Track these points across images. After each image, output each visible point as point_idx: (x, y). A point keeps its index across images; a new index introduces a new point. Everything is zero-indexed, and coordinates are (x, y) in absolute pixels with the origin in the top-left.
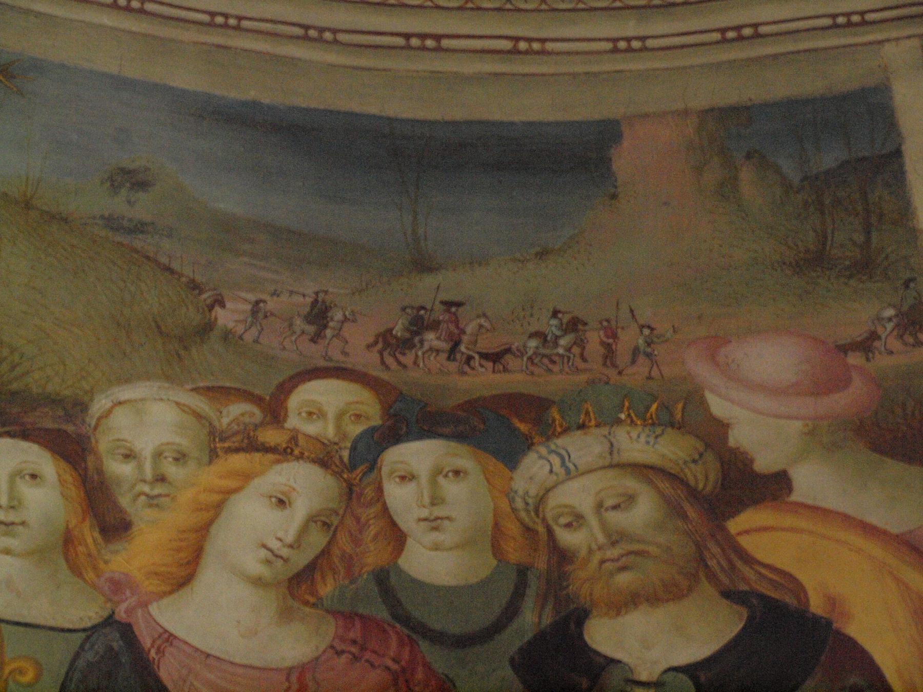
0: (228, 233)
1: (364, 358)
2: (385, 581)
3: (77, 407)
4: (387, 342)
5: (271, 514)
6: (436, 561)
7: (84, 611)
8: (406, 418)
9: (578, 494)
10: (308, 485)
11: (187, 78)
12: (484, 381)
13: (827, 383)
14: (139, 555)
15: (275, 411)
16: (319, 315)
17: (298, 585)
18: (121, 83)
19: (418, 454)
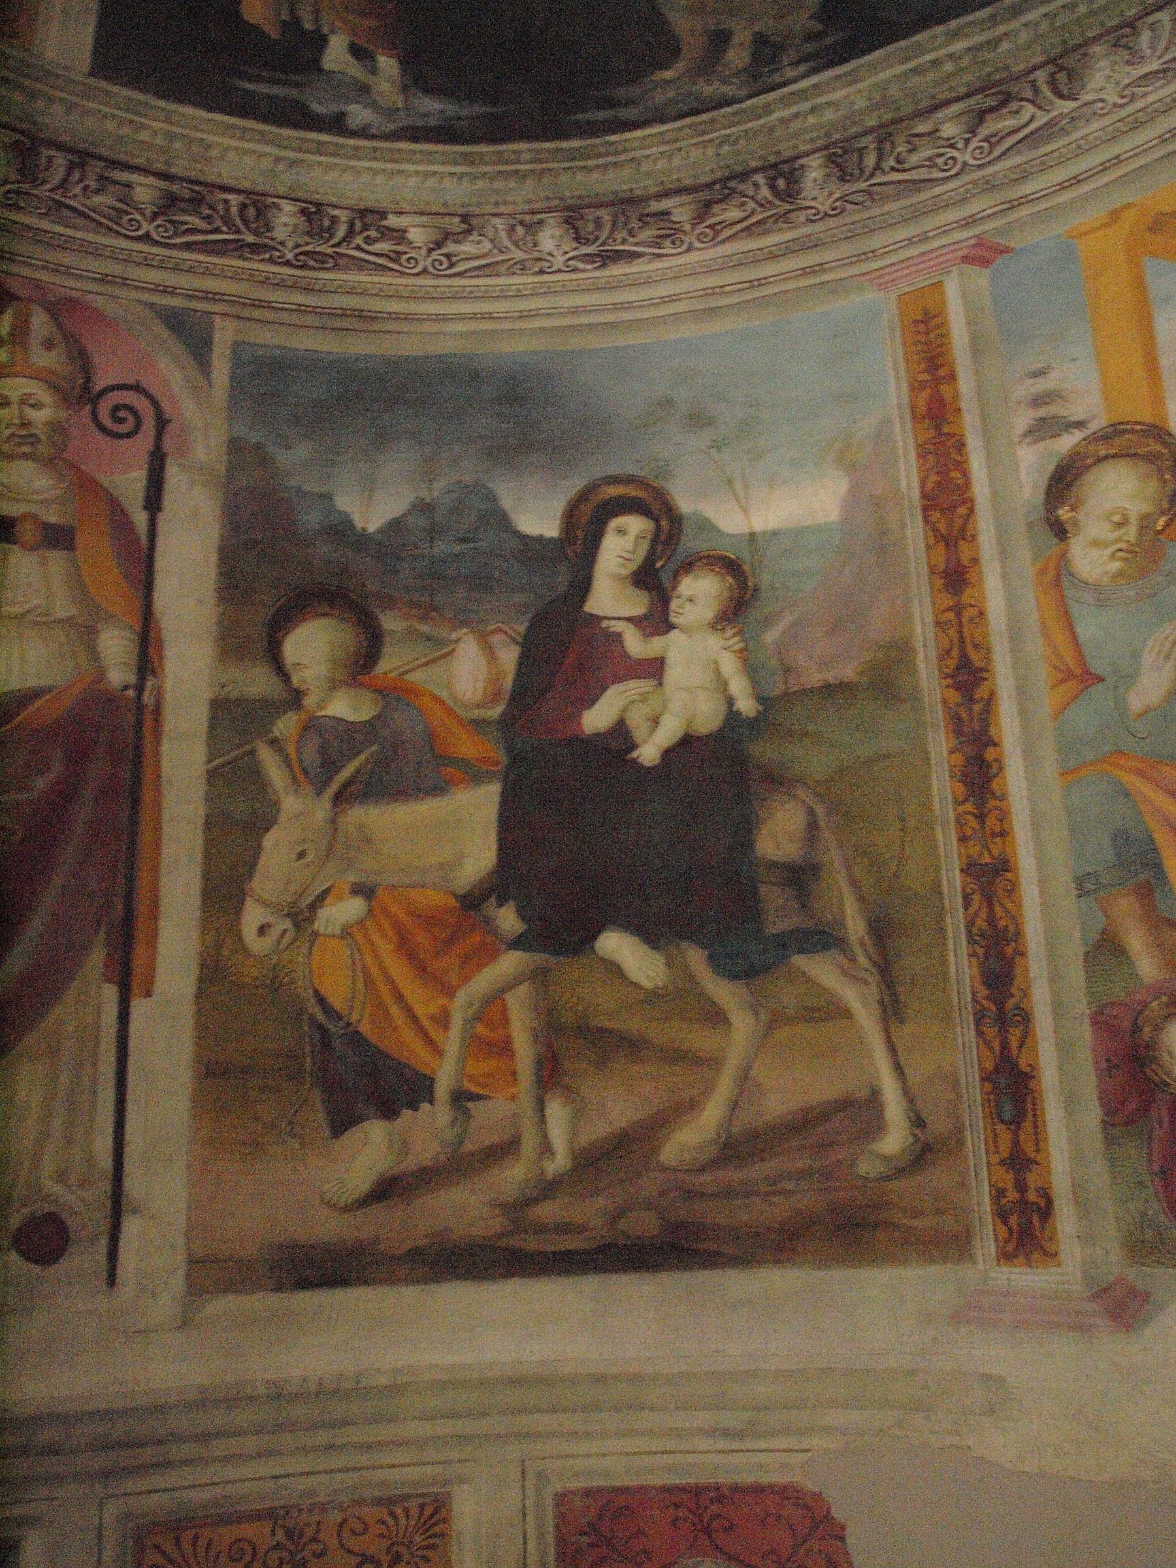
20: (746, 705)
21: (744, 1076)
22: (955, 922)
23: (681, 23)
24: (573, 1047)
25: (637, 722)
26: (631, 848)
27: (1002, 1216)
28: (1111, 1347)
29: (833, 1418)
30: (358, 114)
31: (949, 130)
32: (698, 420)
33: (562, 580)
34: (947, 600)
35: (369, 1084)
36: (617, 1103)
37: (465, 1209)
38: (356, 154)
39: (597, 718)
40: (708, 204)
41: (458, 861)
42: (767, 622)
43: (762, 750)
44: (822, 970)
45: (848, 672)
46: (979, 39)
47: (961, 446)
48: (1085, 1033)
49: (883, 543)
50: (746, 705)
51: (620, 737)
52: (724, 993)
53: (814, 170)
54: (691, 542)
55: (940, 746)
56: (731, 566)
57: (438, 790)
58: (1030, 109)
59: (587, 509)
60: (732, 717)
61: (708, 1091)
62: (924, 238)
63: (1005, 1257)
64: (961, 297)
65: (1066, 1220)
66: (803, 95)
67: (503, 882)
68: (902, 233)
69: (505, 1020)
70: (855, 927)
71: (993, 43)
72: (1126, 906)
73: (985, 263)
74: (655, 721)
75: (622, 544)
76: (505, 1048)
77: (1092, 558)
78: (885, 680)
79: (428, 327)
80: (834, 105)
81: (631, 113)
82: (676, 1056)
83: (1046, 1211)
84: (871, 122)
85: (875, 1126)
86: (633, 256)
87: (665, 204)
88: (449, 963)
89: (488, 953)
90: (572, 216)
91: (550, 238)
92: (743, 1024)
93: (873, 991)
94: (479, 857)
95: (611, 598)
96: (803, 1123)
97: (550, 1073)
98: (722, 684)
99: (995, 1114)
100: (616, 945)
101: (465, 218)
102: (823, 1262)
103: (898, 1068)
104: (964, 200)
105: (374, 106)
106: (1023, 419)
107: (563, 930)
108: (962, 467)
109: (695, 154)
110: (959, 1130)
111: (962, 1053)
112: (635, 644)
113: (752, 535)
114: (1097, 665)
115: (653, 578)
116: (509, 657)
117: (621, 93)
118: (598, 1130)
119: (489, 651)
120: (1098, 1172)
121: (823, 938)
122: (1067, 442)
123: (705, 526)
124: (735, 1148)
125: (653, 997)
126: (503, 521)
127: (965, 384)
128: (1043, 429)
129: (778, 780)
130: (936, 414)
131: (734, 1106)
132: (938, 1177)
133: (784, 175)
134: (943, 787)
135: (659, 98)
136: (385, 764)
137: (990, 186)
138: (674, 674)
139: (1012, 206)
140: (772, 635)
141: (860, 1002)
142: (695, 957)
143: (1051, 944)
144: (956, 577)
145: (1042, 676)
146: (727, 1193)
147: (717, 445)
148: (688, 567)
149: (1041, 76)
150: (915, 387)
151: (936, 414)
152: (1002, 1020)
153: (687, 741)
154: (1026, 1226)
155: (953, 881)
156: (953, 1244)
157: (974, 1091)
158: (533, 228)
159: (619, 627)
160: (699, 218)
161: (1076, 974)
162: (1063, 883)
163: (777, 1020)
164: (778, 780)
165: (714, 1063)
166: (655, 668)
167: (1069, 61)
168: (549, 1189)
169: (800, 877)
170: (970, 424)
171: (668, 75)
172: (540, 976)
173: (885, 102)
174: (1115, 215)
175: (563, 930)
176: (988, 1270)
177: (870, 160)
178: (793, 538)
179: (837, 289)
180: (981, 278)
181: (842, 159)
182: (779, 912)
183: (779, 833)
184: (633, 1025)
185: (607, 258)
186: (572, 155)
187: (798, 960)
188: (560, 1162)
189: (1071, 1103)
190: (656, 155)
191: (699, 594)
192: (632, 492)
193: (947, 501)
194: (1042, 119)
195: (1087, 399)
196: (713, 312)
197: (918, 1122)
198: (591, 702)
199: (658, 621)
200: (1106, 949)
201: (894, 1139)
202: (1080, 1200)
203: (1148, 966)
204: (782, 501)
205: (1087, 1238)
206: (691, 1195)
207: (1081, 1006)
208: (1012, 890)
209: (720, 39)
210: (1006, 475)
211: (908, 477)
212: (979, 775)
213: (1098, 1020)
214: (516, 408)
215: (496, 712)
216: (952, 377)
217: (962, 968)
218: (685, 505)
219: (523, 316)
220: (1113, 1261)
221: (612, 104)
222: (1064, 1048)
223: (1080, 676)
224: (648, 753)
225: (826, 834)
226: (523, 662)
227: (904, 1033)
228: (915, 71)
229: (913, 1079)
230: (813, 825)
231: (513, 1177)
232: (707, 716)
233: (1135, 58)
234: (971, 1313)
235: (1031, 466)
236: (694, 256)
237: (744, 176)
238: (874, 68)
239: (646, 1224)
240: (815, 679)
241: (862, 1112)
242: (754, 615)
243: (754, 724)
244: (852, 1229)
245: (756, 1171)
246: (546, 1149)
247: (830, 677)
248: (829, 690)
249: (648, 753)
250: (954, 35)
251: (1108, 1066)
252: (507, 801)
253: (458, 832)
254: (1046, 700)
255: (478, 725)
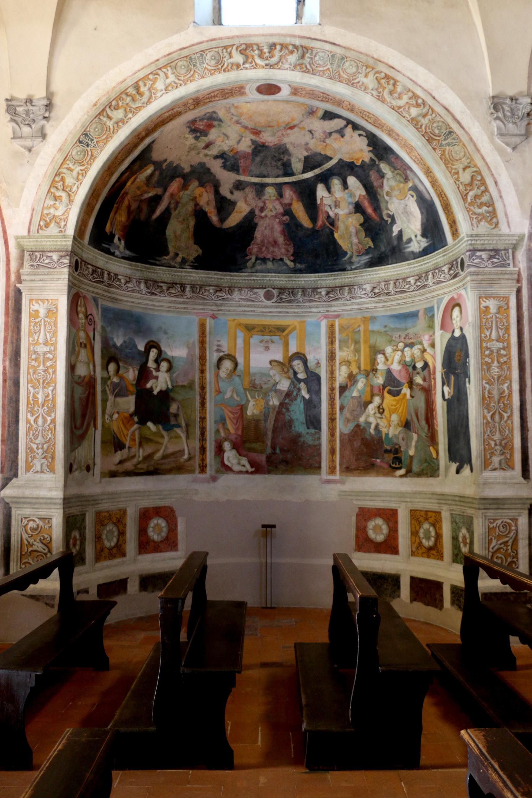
0: (393, 330)
1: (403, 340)
2: (405, 361)
3: (384, 350)
4: (405, 338)
5: (397, 356)
6: (408, 359)
7: (386, 368)
8: (406, 346)
9: (415, 352)
10: (399, 353)
11: (389, 313)
12: (411, 341)
13: (429, 340)
14: (389, 363)
15: (397, 346)
16: (400, 336)
17: (400, 362)
18: (383, 316)
19: (407, 349)
20: (170, 386)
21: (166, 447)
22: (197, 425)
23: (171, 249)
24: (144, 440)
25: (154, 387)
26: (154, 408)
27: (200, 467)
28: (212, 484)
29: (175, 496)
30: (117, 253)
31: (211, 291)
32: (166, 333)
33: (144, 360)
34: (201, 375)
35: (119, 446)
36: (149, 449)
37: (129, 466)
38: (115, 261)
39: (149, 385)
40: (169, 288)
41: (128, 409)
42: (174, 372)
43: (172, 394)
44: (178, 431)
45: (185, 384)
46: (219, 277)
47: (205, 349)
48: (213, 443)
49: (192, 363)
50: (170, 386)
51: (151, 390)
52: (164, 433)
53: (188, 289)
54: (163, 356)
55: (198, 398)
56: (169, 361)
57: (126, 396)
58: (224, 294)
59: (148, 346)
60: (168, 388)
61: (161, 448)
62: (204, 309)
63: (200, 473)
64: (209, 322)
65: (208, 468)
66: (188, 272)
67: (136, 413)
68: (201, 307)
69: (135, 436)
70: (183, 424)
71: (221, 279)
72: (221, 426)
73: (213, 318)
74: (156, 387)
75: (153, 353)
76: (134, 440)
77: (223, 373)
78: (190, 386)
79: (125, 303)
80: (194, 277)
81: (158, 263)
82: (157, 443)
83: (206, 466)
84: (199, 283)
85: (184, 455)
86: (156, 295)
87: (162, 284)
88: (128, 426)
89: (132, 425)
90: (146, 281)
91: (142, 286)
92: (166, 438)
93: (185, 434)
94: (132, 408)
95: (151, 364)
96: (174, 454)
97: (140, 445)
98: (167, 382)
99: (200, 453)
100: (150, 424)
101: (129, 278)
102: (175, 474)
103: (188, 446)
104: (212, 305)
105: (119, 251)
106: (215, 348)
107: (142, 422)
108: (205, 353)
109: (168, 276)
110: (195, 456)
111: (196, 444)
112: (154, 373)
113: (173, 357)
114: (221, 390)
115: (157, 361)
116: (137, 372)
117: (157, 258)
118: (146, 454)
119: (134, 371)
120: (213, 461)
121: (179, 426)
122: (221, 354)
123: (166, 353)
124: (165, 457)
125: (154, 433)
126: (135, 346)
127: (208, 339)
128: (218, 351)
129: (173, 400)
130: (202, 343)
131: (164, 451)
132: (191, 462)
133: (183, 286)
134: (198, 405)
135: (164, 261)
136: (120, 391)
137: (216, 305)
138: (160, 379)
139: (219, 310)
140: (175, 375)
141: (183, 436)
142: (160, 427)
143: (210, 430)
144: (202, 371)
145: (213, 390)
146: (162, 464)
147: (168, 338)
148: (163, 360)
149: (227, 289)
150: (200, 337)
151: (202, 343)
152: (203, 440)
153: (161, 392)
154: (203, 469)
155: (198, 419)
156: (192, 471)
157: (198, 450)
158: (140, 283)
159: (152, 369)
160: (168, 290)
161: (213, 435)
162: (213, 422)
163: (171, 438)
164: (173, 400)
165: (162, 444)
166: (157, 378)
167: (232, 289)
168: (139, 463)
169: (176, 416)
170: (207, 346)
171: (166, 258)
172: (139, 428)
173: (202, 281)
174: (234, 320)
175: (142, 422)
176: (198, 475)
177: (198, 291)
178: (180, 358)
179: (189, 313)
180: (213, 321)
181: (193, 287)
182: (173, 421)
183: (173, 408)
184: (151, 437)
185: (152, 294)
186: (147, 268)
187: (175, 429)
188: (141, 459)
189: (210, 452)
190: (161, 273)
191: (164, 365)
192: (155, 344)
193: (202, 358)
194: (226, 297)
195: (226, 349)
196: (169, 311)
197: (189, 454)
198: (147, 382)
199: (158, 369)
200: (217, 431)
201: (186, 457)
202: (210, 466)
203: (223, 434)
204: (177, 351)
205: (211, 470)
206: (158, 464)
207: (213, 439)
208: (206, 421)
209: (177, 255)
210: (212, 357)
211: (197, 352)
212: (203, 404)
213: (216, 441)
214: (135, 322)
215: (135, 383)
216: (206, 337)
217: (198, 432)
218: (163, 349)
219: (139, 303)
220: (213, 473)
221: (156, 260)
222: (211, 444)
223: (219, 392)
224: (155, 393)
225: (180, 409)
226: (139, 373)
227: (189, 442)
228: (208, 277)
229: (190, 447)
230: (178, 408)
231: (135, 461)
232: (164, 388)
233: (241, 294)
234: (195, 481)
235: (216, 356)
236: (167, 298)
237: (176, 284)
238: (202, 273)
239: (152, 468)
240: (181, 384)
241: (182, 452)
242: (172, 371)
243: (172, 390)
244: (179, 469)
245: (167, 461)
246: (139, 457)
247: (183, 384)
248: (183, 386)
249: (155, 393)
250: (215, 274)
251: (216, 447)
252: (136, 398)
253: (129, 403)
254: (213, 394)
255: (132, 384)
